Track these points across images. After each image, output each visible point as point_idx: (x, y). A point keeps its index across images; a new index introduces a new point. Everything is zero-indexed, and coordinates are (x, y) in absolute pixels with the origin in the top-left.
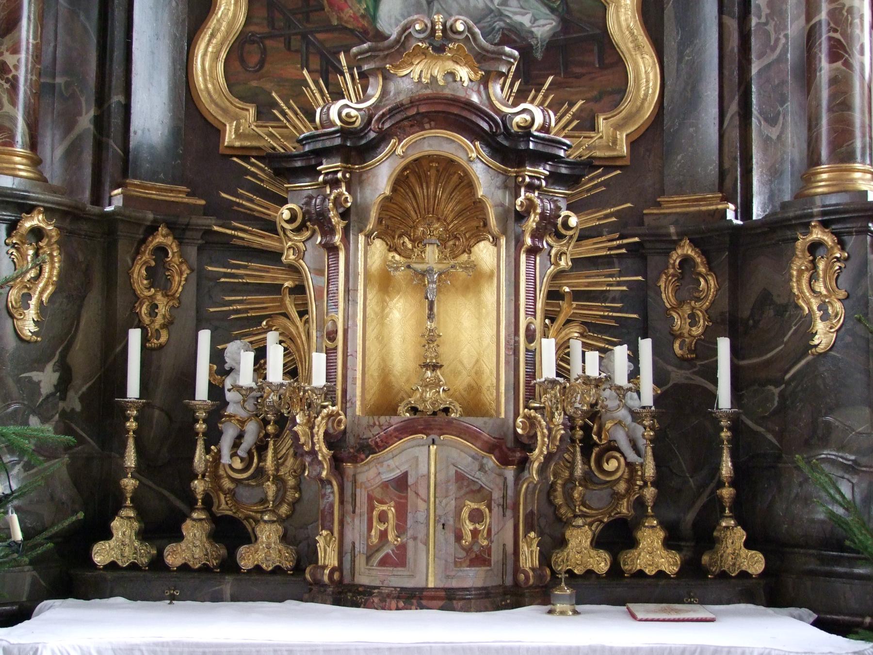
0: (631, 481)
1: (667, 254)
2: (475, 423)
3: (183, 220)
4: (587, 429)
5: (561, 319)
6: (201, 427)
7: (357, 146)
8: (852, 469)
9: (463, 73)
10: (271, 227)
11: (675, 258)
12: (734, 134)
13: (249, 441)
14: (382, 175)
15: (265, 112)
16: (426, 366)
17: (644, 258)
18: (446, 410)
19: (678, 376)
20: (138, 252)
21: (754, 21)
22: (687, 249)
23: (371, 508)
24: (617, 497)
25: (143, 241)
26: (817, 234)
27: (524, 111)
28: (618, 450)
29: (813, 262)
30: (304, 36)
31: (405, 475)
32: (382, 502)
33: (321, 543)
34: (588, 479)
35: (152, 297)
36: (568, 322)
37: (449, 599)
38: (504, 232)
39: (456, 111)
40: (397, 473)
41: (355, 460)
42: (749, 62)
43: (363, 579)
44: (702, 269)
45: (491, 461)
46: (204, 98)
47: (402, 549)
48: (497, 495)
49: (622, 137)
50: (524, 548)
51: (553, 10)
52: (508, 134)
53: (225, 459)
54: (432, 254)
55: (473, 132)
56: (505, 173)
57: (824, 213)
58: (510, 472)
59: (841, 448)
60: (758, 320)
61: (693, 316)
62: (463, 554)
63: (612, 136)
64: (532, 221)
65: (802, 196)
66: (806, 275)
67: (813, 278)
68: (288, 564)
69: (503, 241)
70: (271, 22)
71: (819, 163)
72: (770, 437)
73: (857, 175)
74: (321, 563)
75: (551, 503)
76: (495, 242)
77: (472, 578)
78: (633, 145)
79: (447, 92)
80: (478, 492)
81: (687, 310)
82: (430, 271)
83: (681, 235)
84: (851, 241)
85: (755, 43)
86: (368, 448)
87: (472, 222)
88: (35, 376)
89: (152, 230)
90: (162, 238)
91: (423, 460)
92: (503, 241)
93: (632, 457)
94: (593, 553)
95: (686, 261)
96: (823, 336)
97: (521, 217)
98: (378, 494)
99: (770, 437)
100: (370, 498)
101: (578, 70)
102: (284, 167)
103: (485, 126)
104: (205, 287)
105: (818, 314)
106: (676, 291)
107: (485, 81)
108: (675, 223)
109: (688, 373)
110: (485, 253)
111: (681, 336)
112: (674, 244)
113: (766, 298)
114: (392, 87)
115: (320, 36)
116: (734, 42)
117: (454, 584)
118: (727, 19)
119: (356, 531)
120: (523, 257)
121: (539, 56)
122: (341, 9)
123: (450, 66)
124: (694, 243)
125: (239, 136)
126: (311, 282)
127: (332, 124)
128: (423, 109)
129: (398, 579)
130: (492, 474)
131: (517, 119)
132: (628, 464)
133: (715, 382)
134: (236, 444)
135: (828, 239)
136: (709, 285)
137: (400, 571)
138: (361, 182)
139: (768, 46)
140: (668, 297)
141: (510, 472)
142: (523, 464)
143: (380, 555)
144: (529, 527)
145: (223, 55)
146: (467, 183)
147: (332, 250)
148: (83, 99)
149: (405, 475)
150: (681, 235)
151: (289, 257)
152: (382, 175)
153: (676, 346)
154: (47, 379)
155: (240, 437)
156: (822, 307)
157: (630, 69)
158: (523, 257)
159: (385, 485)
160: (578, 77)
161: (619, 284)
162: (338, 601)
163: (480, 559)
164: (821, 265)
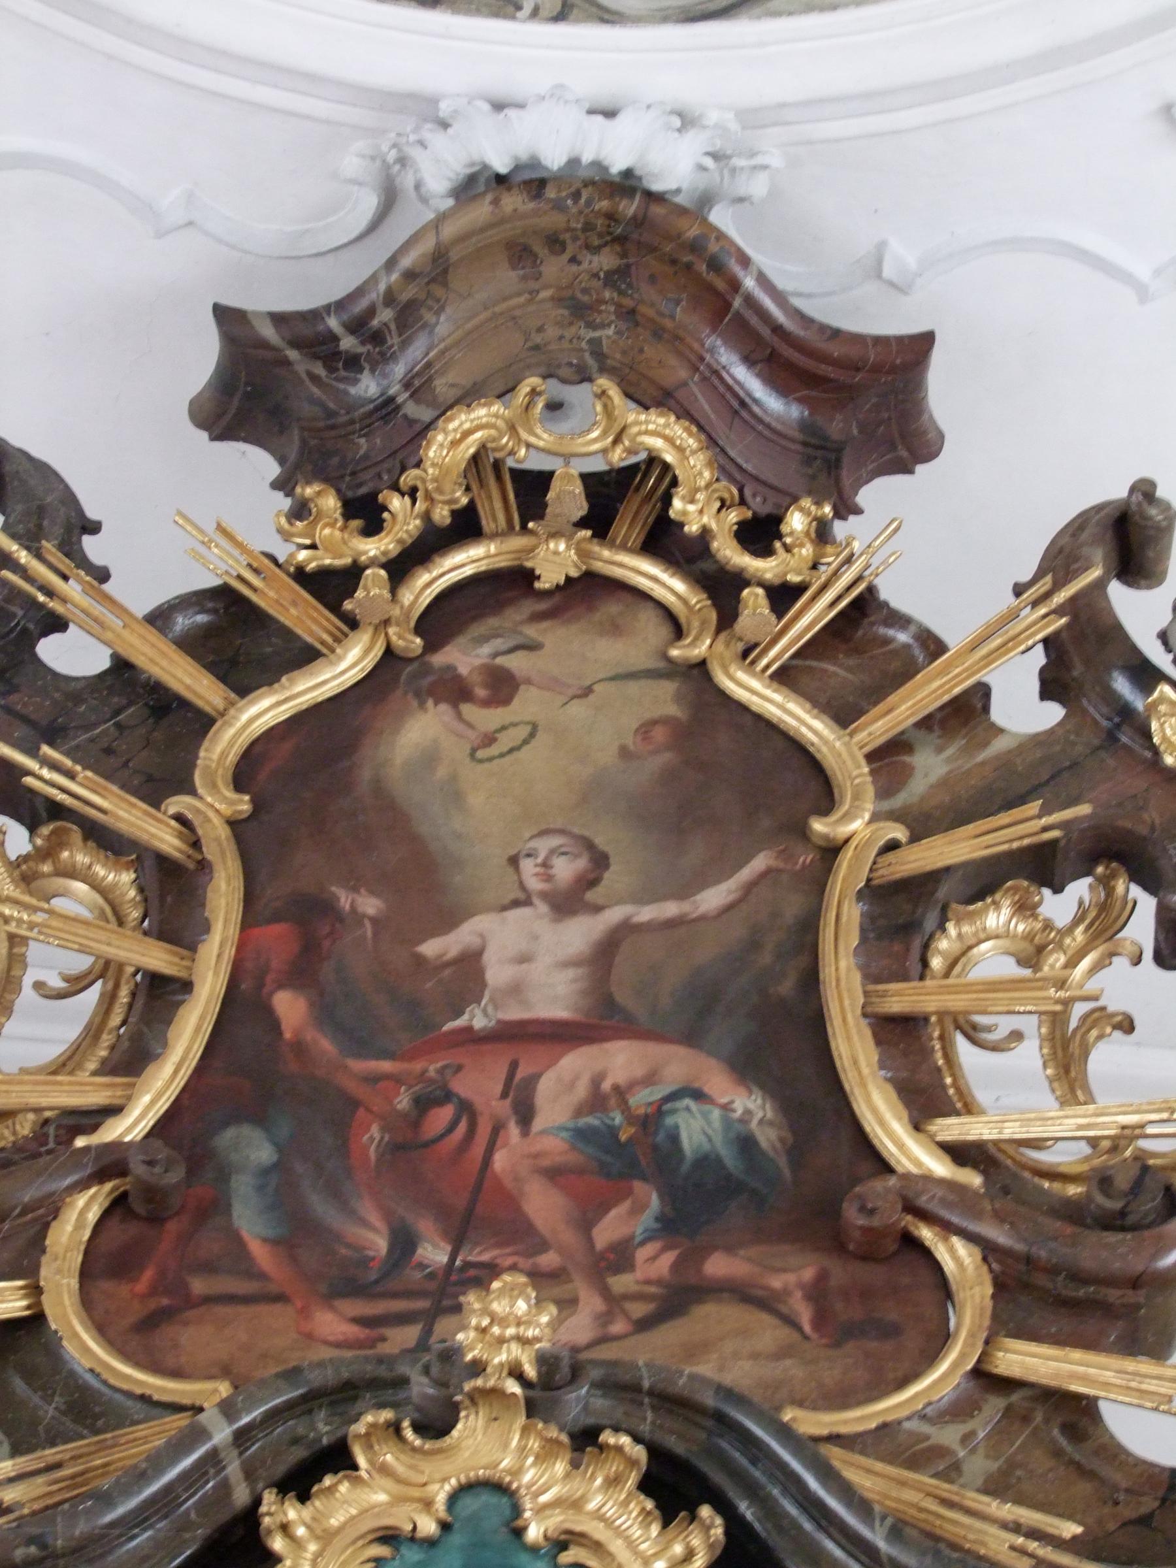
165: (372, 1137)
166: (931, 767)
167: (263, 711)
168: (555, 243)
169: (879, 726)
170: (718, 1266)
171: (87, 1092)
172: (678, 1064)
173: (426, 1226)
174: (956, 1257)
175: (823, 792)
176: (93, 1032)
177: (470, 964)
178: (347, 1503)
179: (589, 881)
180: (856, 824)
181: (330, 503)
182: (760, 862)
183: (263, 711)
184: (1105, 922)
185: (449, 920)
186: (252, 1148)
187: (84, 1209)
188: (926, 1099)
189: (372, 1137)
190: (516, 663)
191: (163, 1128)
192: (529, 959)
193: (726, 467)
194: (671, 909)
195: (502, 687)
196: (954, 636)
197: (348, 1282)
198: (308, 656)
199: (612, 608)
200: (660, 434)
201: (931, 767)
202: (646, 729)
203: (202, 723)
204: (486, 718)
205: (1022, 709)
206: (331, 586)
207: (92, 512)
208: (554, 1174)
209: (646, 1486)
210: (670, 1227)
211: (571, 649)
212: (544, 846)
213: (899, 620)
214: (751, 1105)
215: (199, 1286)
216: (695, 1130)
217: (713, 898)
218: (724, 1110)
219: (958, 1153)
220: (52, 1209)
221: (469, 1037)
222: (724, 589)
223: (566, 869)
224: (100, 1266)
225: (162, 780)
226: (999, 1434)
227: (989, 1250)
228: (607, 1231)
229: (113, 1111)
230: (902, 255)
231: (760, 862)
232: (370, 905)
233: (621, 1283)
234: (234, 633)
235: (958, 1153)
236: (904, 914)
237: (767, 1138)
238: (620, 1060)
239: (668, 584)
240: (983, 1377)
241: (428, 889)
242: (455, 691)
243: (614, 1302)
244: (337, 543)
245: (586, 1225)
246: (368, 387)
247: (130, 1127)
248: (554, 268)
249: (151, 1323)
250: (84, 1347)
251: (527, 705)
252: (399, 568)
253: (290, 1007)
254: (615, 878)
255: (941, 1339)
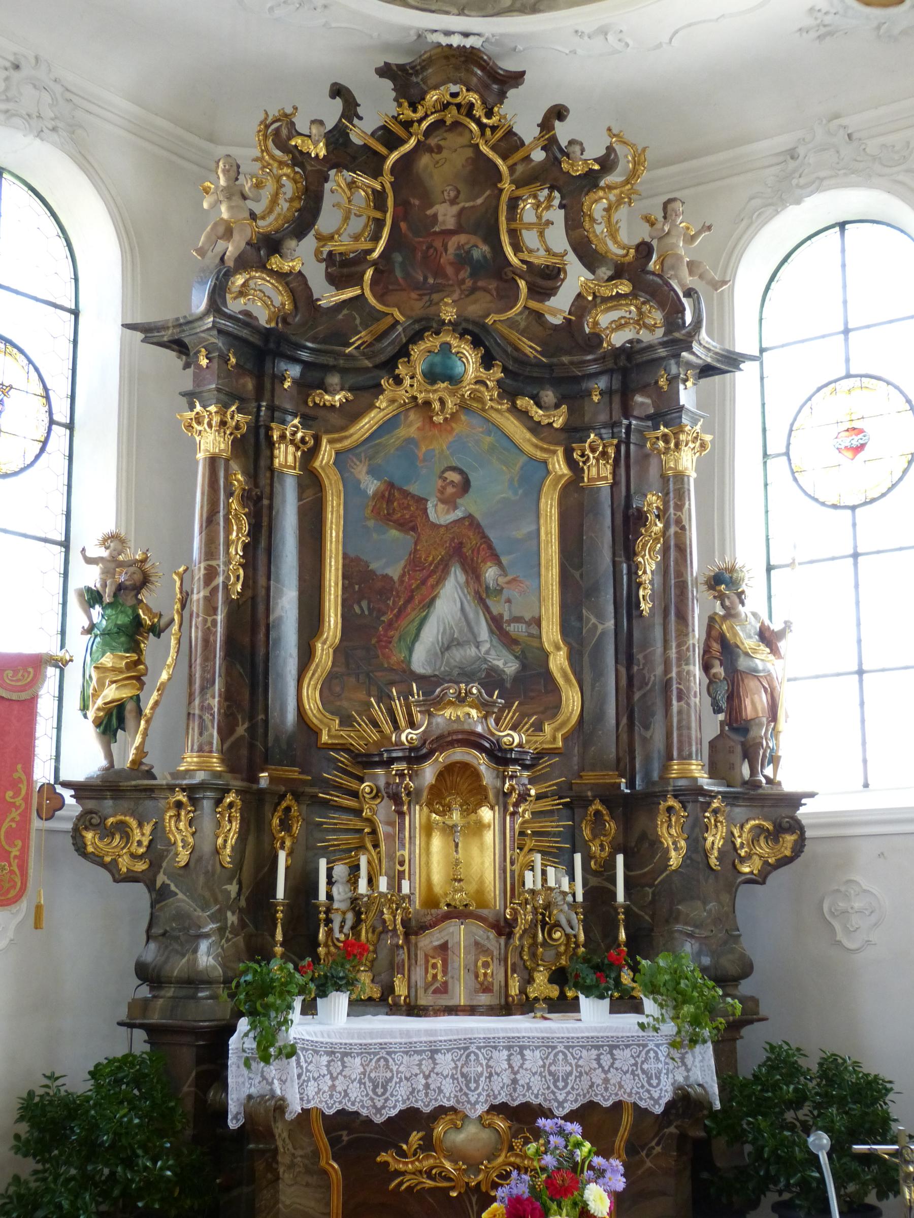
0: (567, 945)
1: (586, 807)
2: (485, 912)
3: (301, 790)
4: (543, 915)
5: (526, 849)
6: (322, 916)
7: (416, 756)
8: (690, 936)
9: (474, 713)
10: (355, 794)
11: (592, 809)
12: (624, 737)
13: (349, 923)
14: (429, 773)
15: (347, 721)
16: (455, 880)
17: (572, 809)
18: (466, 905)
19: (594, 881)
20: (275, 810)
21: (636, 668)
22: (597, 806)
23: (427, 962)
24: (559, 955)
25: (279, 804)
26: (671, 802)
27: (508, 735)
28: (560, 926)
29: (669, 817)
30: (368, 675)
31: (446, 943)
32: (433, 958)
33: (397, 983)
34: (544, 944)
35: (283, 838)
36: (531, 850)
37: (472, 1010)
38: (497, 804)
39: (473, 738)
40: (442, 941)
41: (416, 934)
42: (633, 693)
43: (423, 1001)
44: (607, 818)
45: (492, 934)
46: (309, 712)
47: (445, 984)
48: (496, 953)
49: (559, 736)
50: (510, 982)
51: (516, 657)
52: (500, 749)
53: (337, 935)
54: (456, 816)
55: (481, 749)
56: (497, 770)
57: (674, 791)
58: (502, 940)
59: (686, 924)
60: (641, 849)
61: (602, 845)
62: (478, 986)
63: (552, 734)
64: (514, 797)
65: (664, 779)
66: (666, 825)
67: (669, 826)
68: (376, 995)
69: (497, 808)
70: (347, 665)
71: (672, 759)
72: (647, 918)
73: (694, 767)
74: (397, 993)
75: (522, 958)
76: (492, 808)
77: (484, 999)
78: (565, 739)
79: (466, 727)
80: (487, 952)
81: (597, 842)
82: (455, 826)
83: (595, 797)
84: (690, 806)
85: (636, 682)
86: (423, 928)
87: (476, 795)
88: (228, 887)
89: (283, 797)
90: (289, 801)
91: (459, 934)
92: (497, 808)
93: (569, 930)
94: (549, 986)
95: (597, 813)
96: (675, 860)
97: (507, 795)
98: (431, 953)
99: (647, 918)
100: (426, 956)
101: (532, 694)
102: (366, 761)
103: (487, 745)
104: (312, 827)
105: (672, 847)
106: (592, 830)
107: (485, 717)
108: (591, 790)
109: (599, 880)
110: (486, 814)
111: (595, 857)
112: (591, 802)
113: (643, 837)
114: (434, 721)
115: (378, 674)
116: (624, 682)
117: (475, 1003)
118: (619, 667)
119: (418, 974)
120: (508, 818)
121: (508, 685)
122: (389, 657)
123: (467, 709)
124: (603, 802)
125: (330, 736)
126: (382, 829)
127: (403, 744)
128: (455, 737)
129: (444, 1001)
130: (491, 939)
131: (505, 739)
132: (567, 935)
133: (615, 885)
134: (342, 927)
135: (677, 805)
136: (611, 826)
137: (444, 996)
138: (417, 775)
139: (644, 683)
140: (587, 833)
141: (502, 940)
142: (510, 936)
143: (433, 988)
144: (514, 971)
145: (319, 686)
146: (476, 775)
147: (401, 814)
148: (239, 717)
149: (446, 943)
150: (595, 797)
151: (366, 813)
152: (429, 773)
153: (592, 863)
154: (233, 888)
155: (344, 921)
156: (674, 843)
157: (563, 695)
158: (508, 818)
159: (435, 948)
160: (532, 698)
161: (557, 826)
162: (409, 1015)
163: (486, 989)
164: (673, 819)
165: (419, 255)
166: (520, 169)
167: (394, 156)
168: (453, 56)
169: (510, 162)
170: (480, 284)
171: (368, 246)
172: (474, 239)
173: (429, 275)
174: (522, 284)
175: (499, 177)
176: (366, 226)
177: (435, 216)
178: (423, 346)
179: (457, 197)
180: (506, 186)
181: (406, 104)
182: (488, 193)
183: (394, 156)
184: (550, 198)
185: (431, 206)
186: (398, 258)
187: (369, 273)
188: (517, 248)
189: (419, 255)
190: (442, 143)
191: (382, 255)
192: (446, 214)
193: (484, 102)
194: (471, 204)
195: (440, 149)
196: (527, 142)
197: (416, 287)
198: (403, 142)
199: (460, 129)
200: (473, 97)
201: (520, 169)
202: (467, 160)
203: (384, 158)
204: (437, 157)
205: (539, 156)
206: (407, 125)
207: (359, 102)
208: (451, 264)
209: (472, 343)
210: (472, 275)
211: (453, 140)
212: (448, 188)
213: (515, 134)
214: (485, 248)
215: (391, 287)
216: (476, 254)
217: (479, 201)
218: (481, 250)
219: (523, 261)
220: (364, 273)
221: (435, 233)
222: (483, 127)
223: (452, 194)
224: (374, 282)
225: (376, 173)
226: (527, 317)
227: (527, 283)
228: (462, 275)
229: (372, 251)
230: (520, 47)
231: (488, 193)
232: (417, 202)
233: (463, 287)
234: (390, 139)
235: (523, 261)
236: (514, 203)
237: (489, 256)
238: (462, 238)
239: (474, 126)
240: (525, 307)
241: (428, 201)
242: (430, 150)
243: (462, 291)
244: (408, 114)
245: (457, 274)
246: (414, 79)
247: (376, 255)
248: (453, 60)
249: (383, 295)
250: (372, 300)
251: (445, 154)
252: (420, 121)
253: (403, 225)
254: (462, 196)
255: (517, 299)
